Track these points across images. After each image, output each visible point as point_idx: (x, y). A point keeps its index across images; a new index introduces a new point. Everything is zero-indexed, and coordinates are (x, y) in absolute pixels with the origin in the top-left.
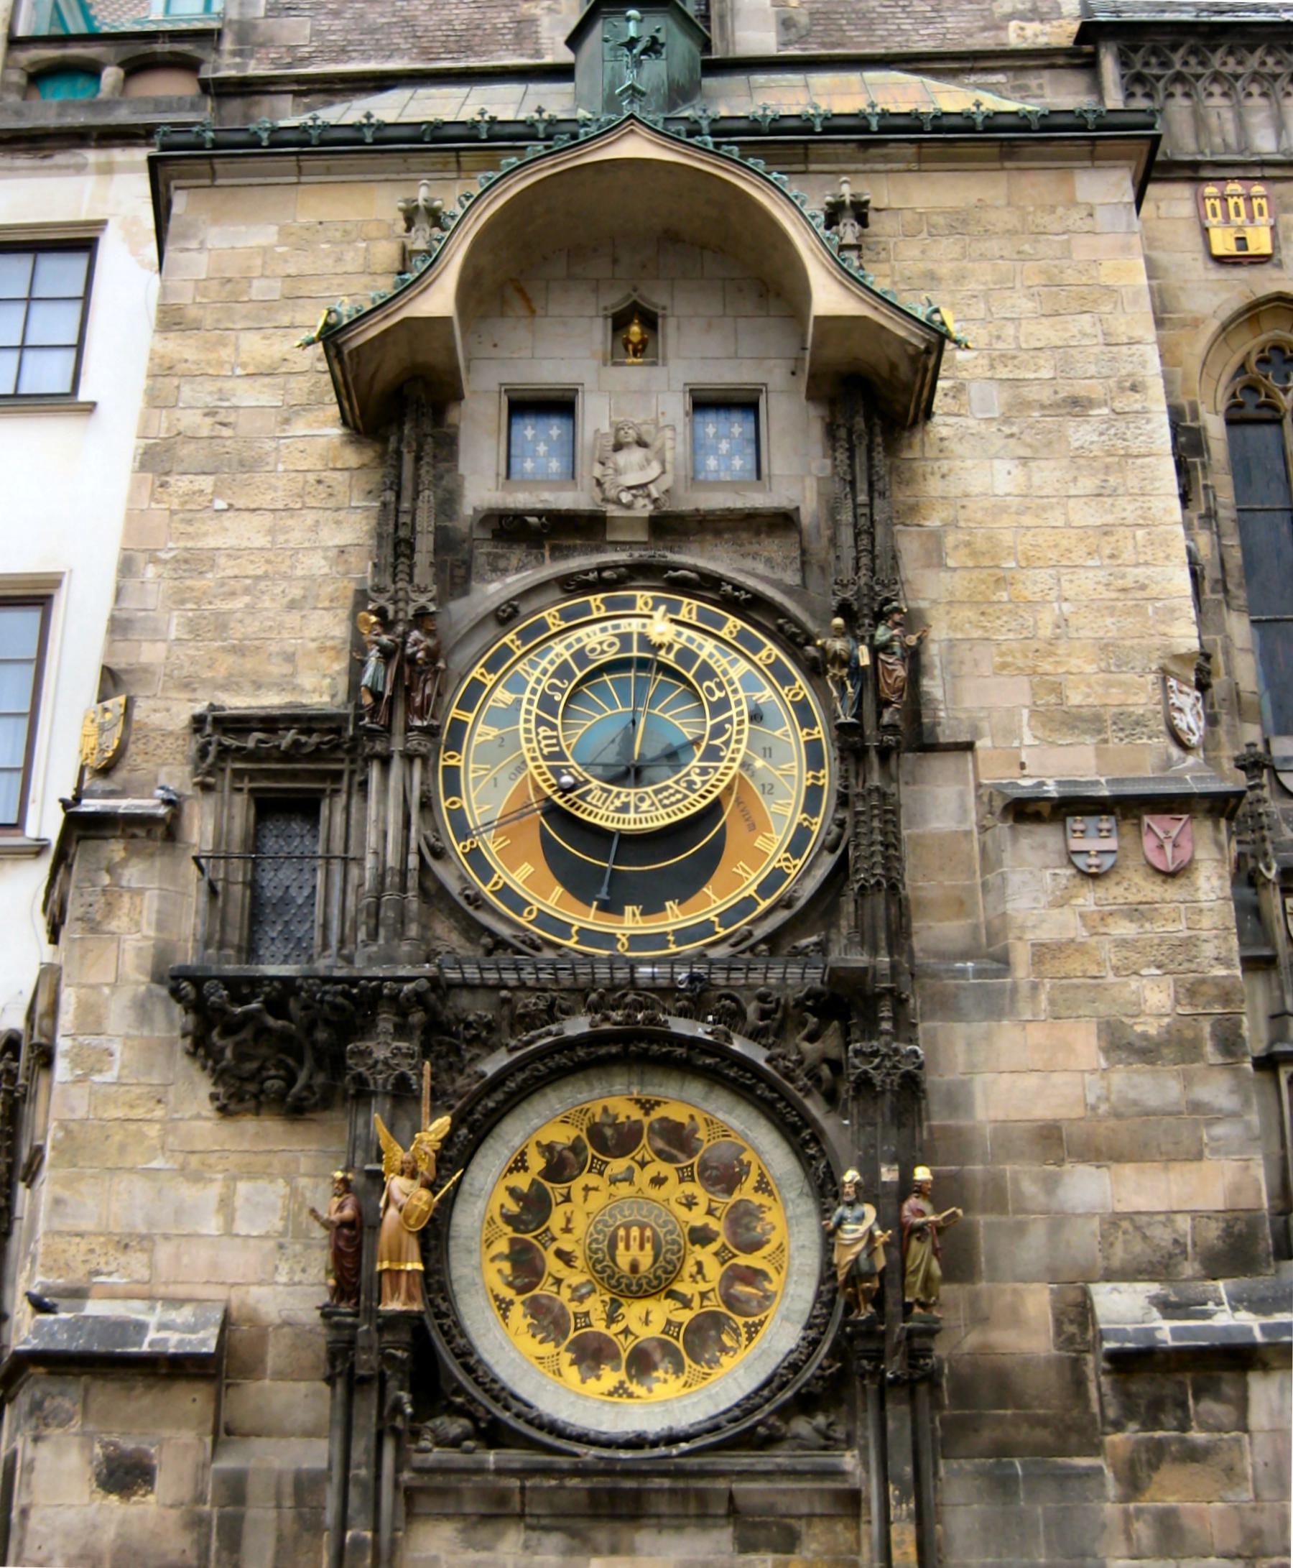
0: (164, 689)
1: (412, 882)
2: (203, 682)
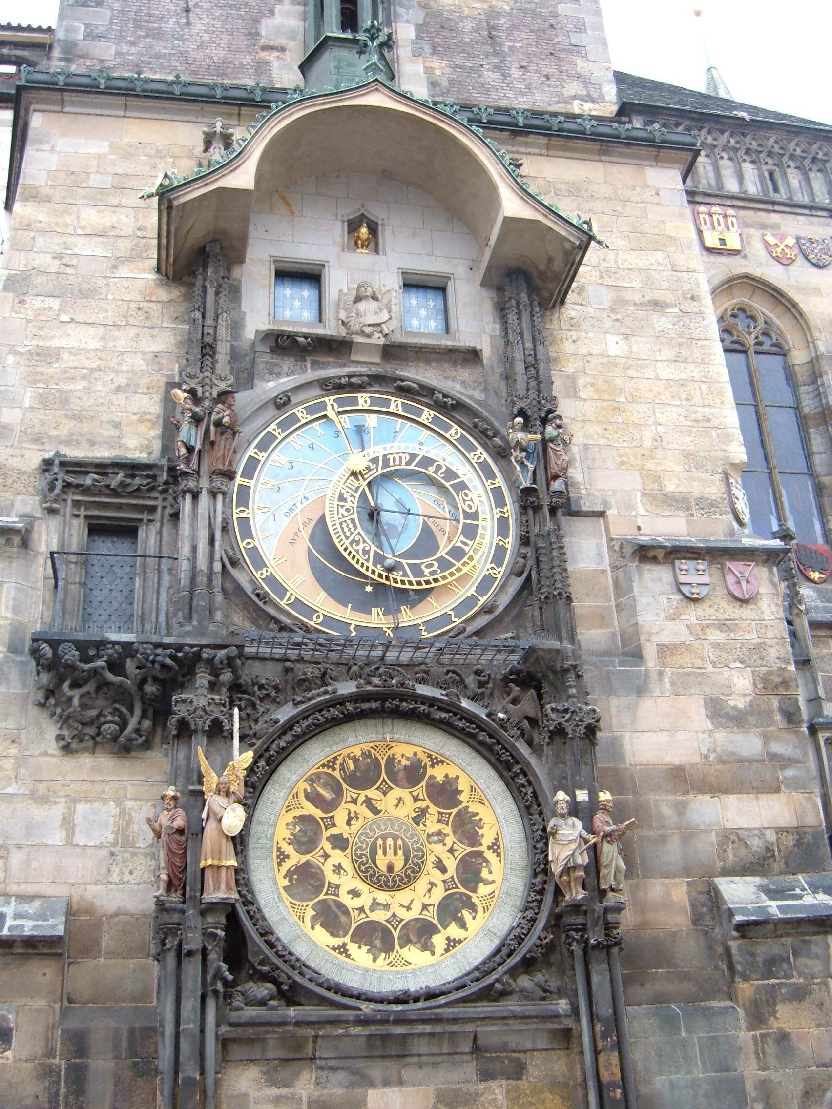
0: (19, 442)
1: (217, 581)
2: (50, 437)
